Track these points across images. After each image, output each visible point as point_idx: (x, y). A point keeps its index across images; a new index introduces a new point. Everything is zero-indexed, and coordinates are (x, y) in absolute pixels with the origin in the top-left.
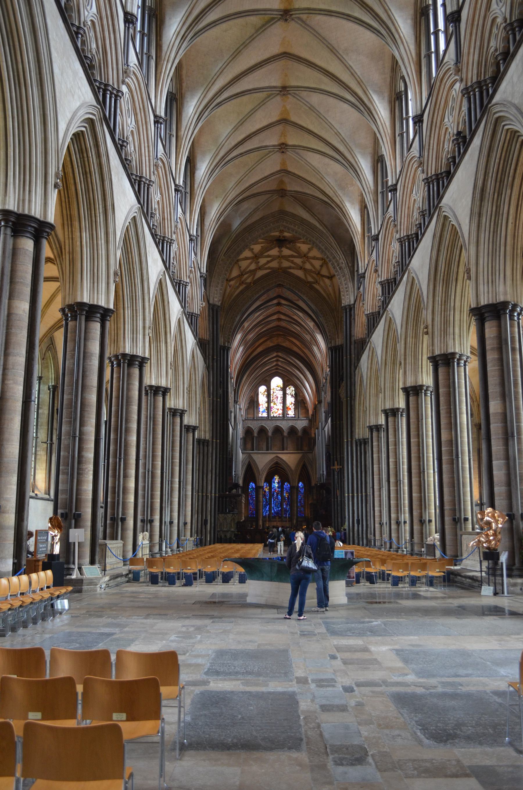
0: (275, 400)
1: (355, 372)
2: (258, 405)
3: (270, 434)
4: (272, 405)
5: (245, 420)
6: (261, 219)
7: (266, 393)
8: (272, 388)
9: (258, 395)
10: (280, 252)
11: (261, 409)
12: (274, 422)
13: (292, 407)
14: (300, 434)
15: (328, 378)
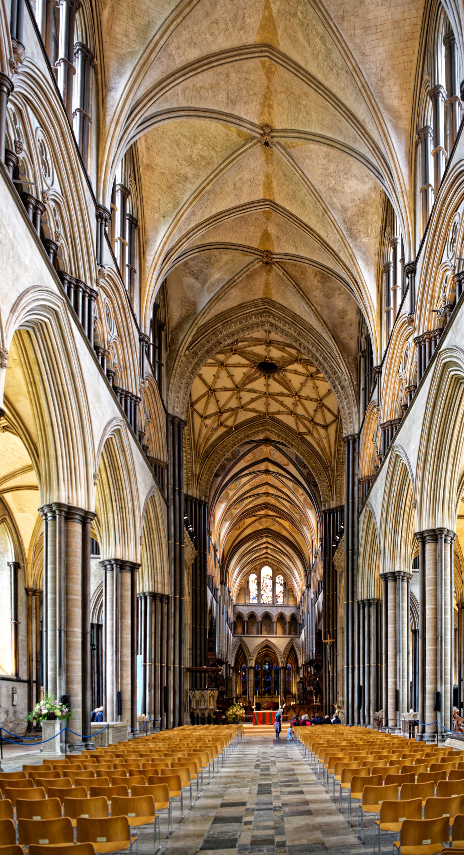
0: (265, 588)
1: (358, 519)
2: (249, 592)
3: (259, 619)
4: (262, 592)
5: (236, 605)
6: (241, 306)
7: (256, 581)
8: (262, 577)
9: (248, 582)
10: (267, 385)
11: (252, 597)
12: (263, 608)
13: (281, 595)
14: (288, 620)
15: (319, 555)
